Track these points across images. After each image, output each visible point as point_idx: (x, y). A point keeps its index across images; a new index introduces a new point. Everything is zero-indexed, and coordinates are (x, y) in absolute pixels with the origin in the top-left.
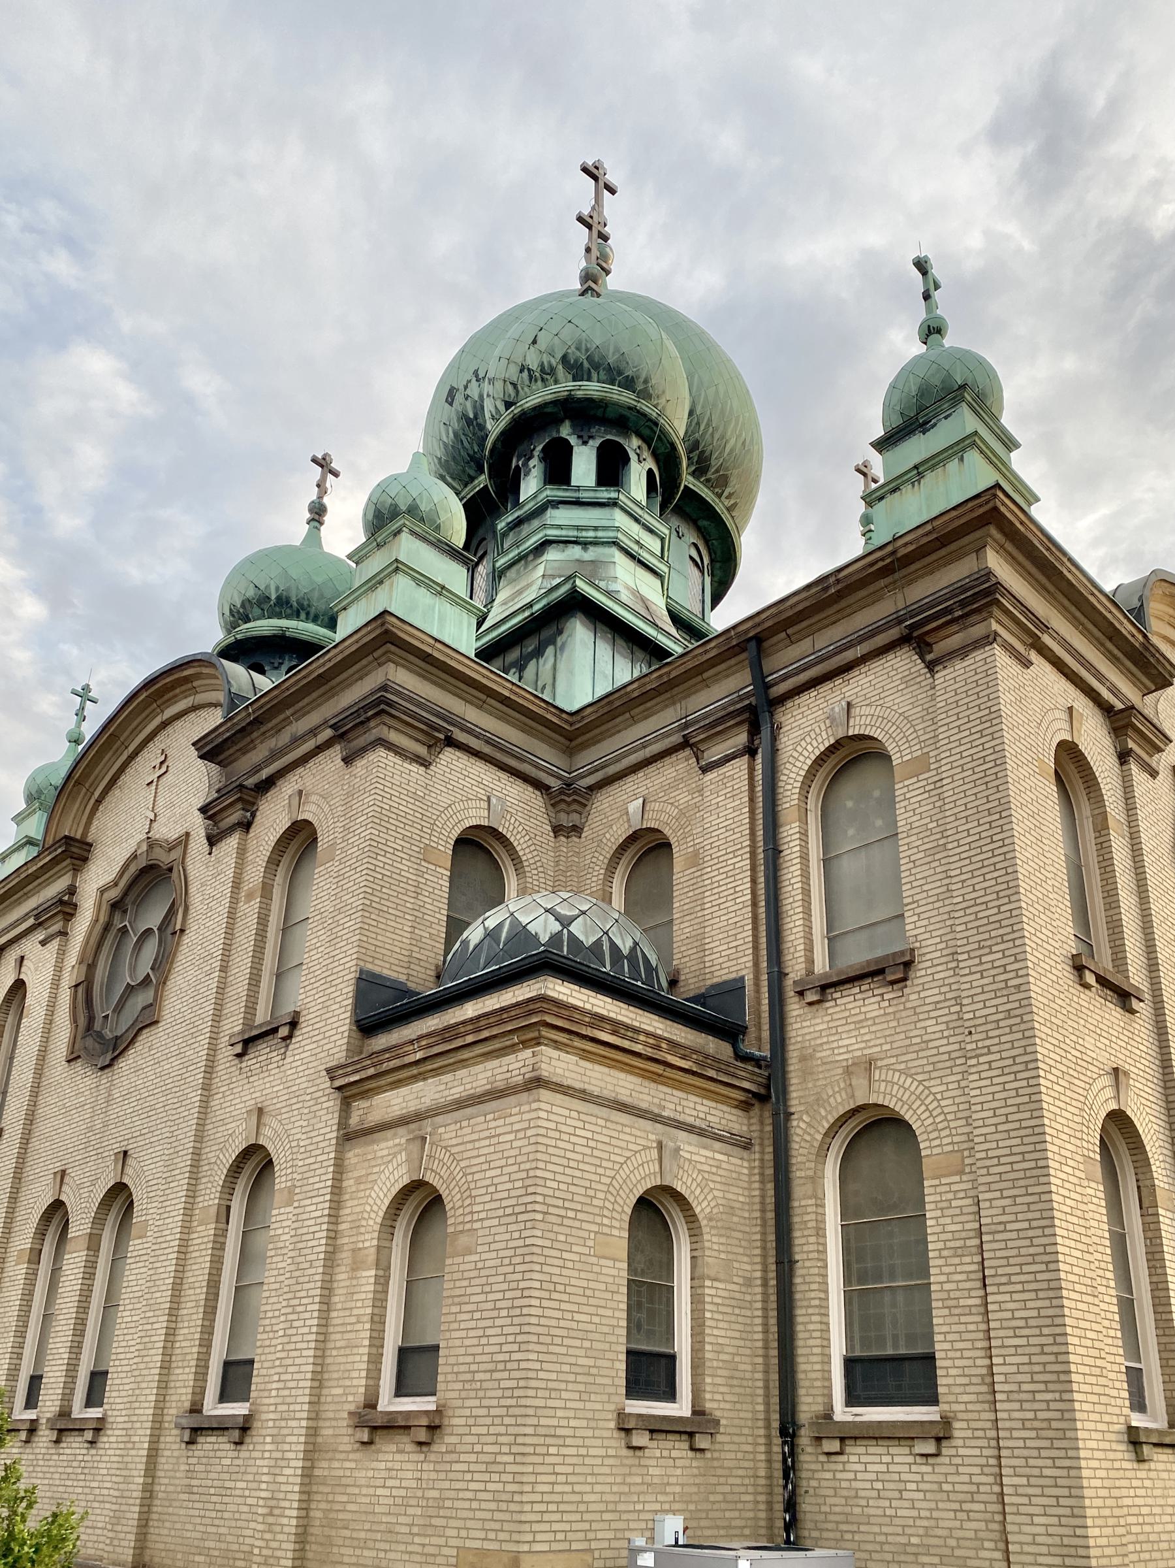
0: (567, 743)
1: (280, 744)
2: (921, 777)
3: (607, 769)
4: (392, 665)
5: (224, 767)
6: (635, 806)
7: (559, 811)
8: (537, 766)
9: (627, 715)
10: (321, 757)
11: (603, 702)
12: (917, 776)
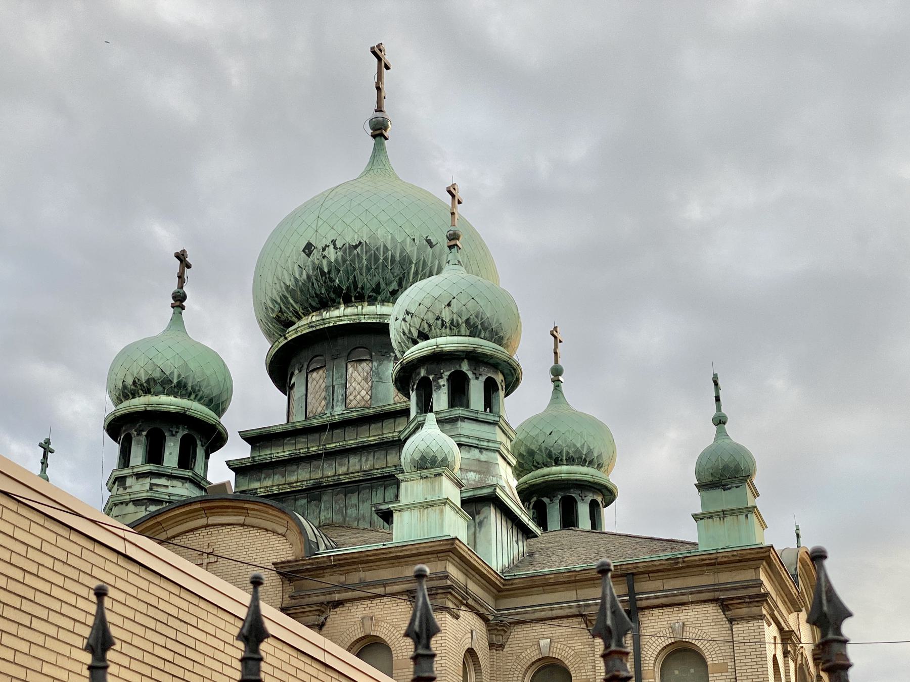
0: (497, 593)
1: (349, 582)
2: (723, 674)
3: (524, 615)
4: (448, 562)
5: (290, 580)
6: (544, 642)
7: (492, 634)
8: (487, 610)
9: (541, 588)
10: (386, 599)
11: (528, 579)
12: (721, 673)
